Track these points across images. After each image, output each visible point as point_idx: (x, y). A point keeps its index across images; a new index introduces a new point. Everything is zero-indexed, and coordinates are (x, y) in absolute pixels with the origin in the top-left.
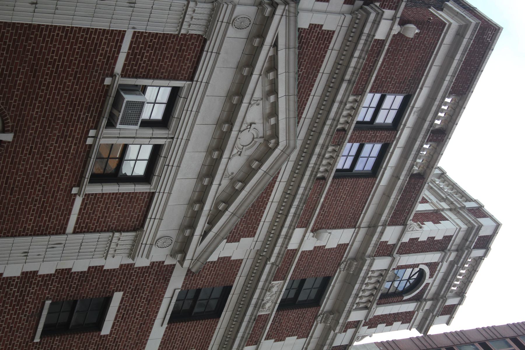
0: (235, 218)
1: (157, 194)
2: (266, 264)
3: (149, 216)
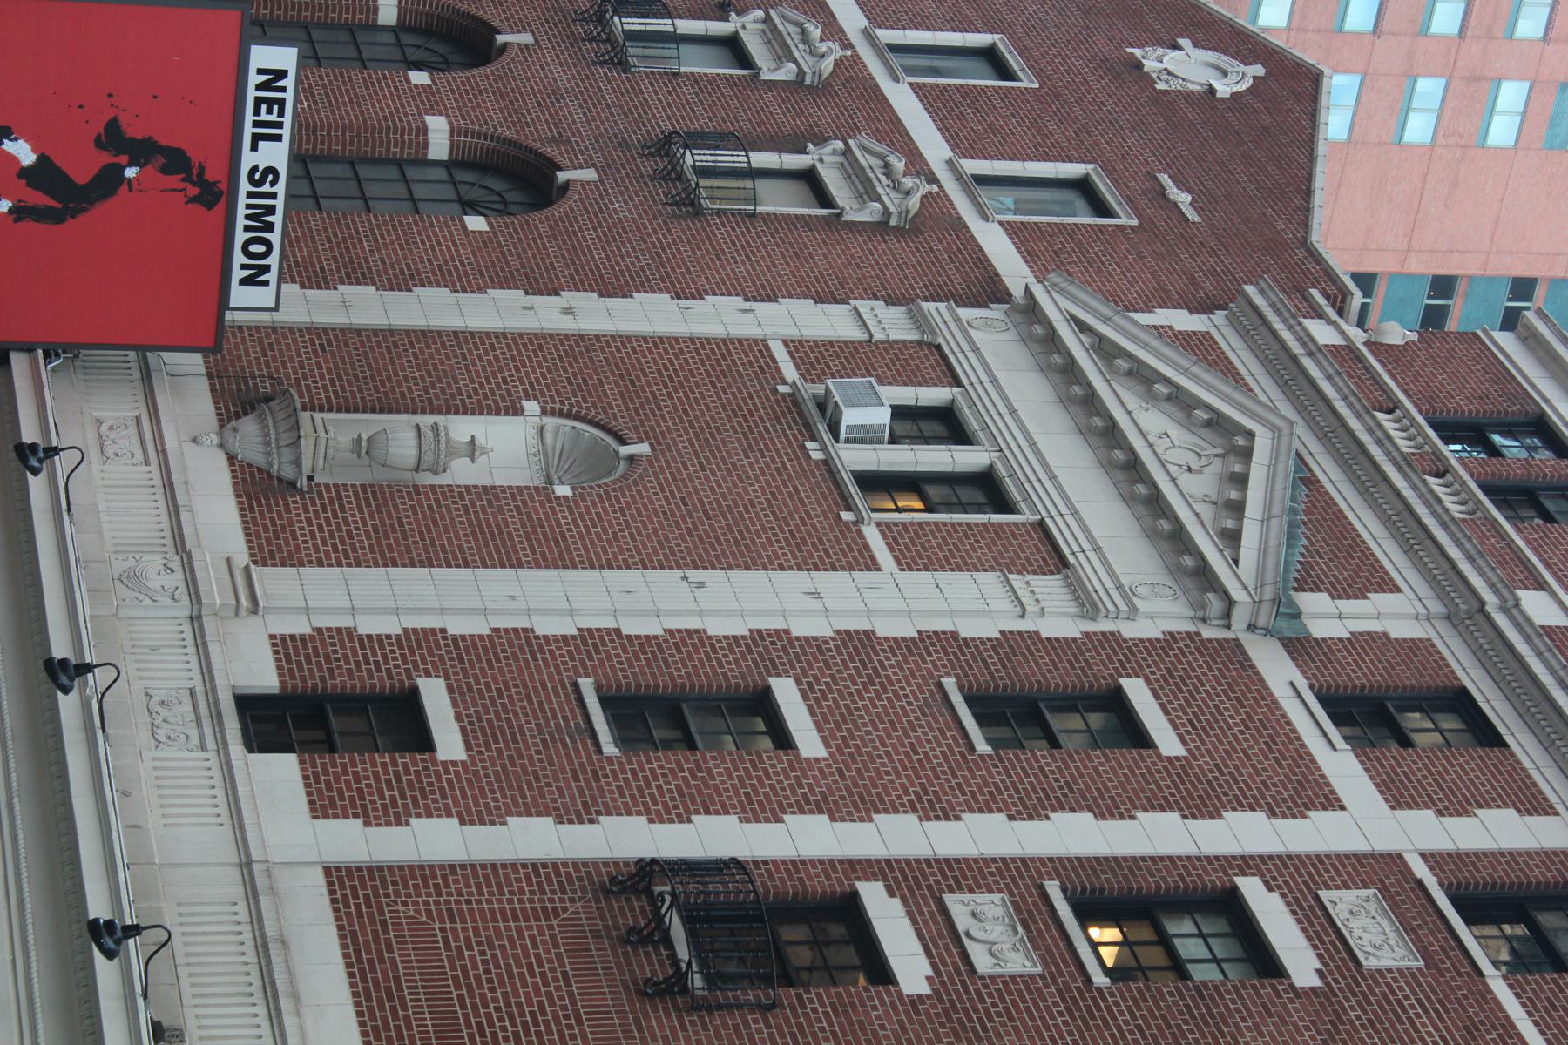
0: (1274, 522)
1: (1049, 522)
2: (1488, 617)
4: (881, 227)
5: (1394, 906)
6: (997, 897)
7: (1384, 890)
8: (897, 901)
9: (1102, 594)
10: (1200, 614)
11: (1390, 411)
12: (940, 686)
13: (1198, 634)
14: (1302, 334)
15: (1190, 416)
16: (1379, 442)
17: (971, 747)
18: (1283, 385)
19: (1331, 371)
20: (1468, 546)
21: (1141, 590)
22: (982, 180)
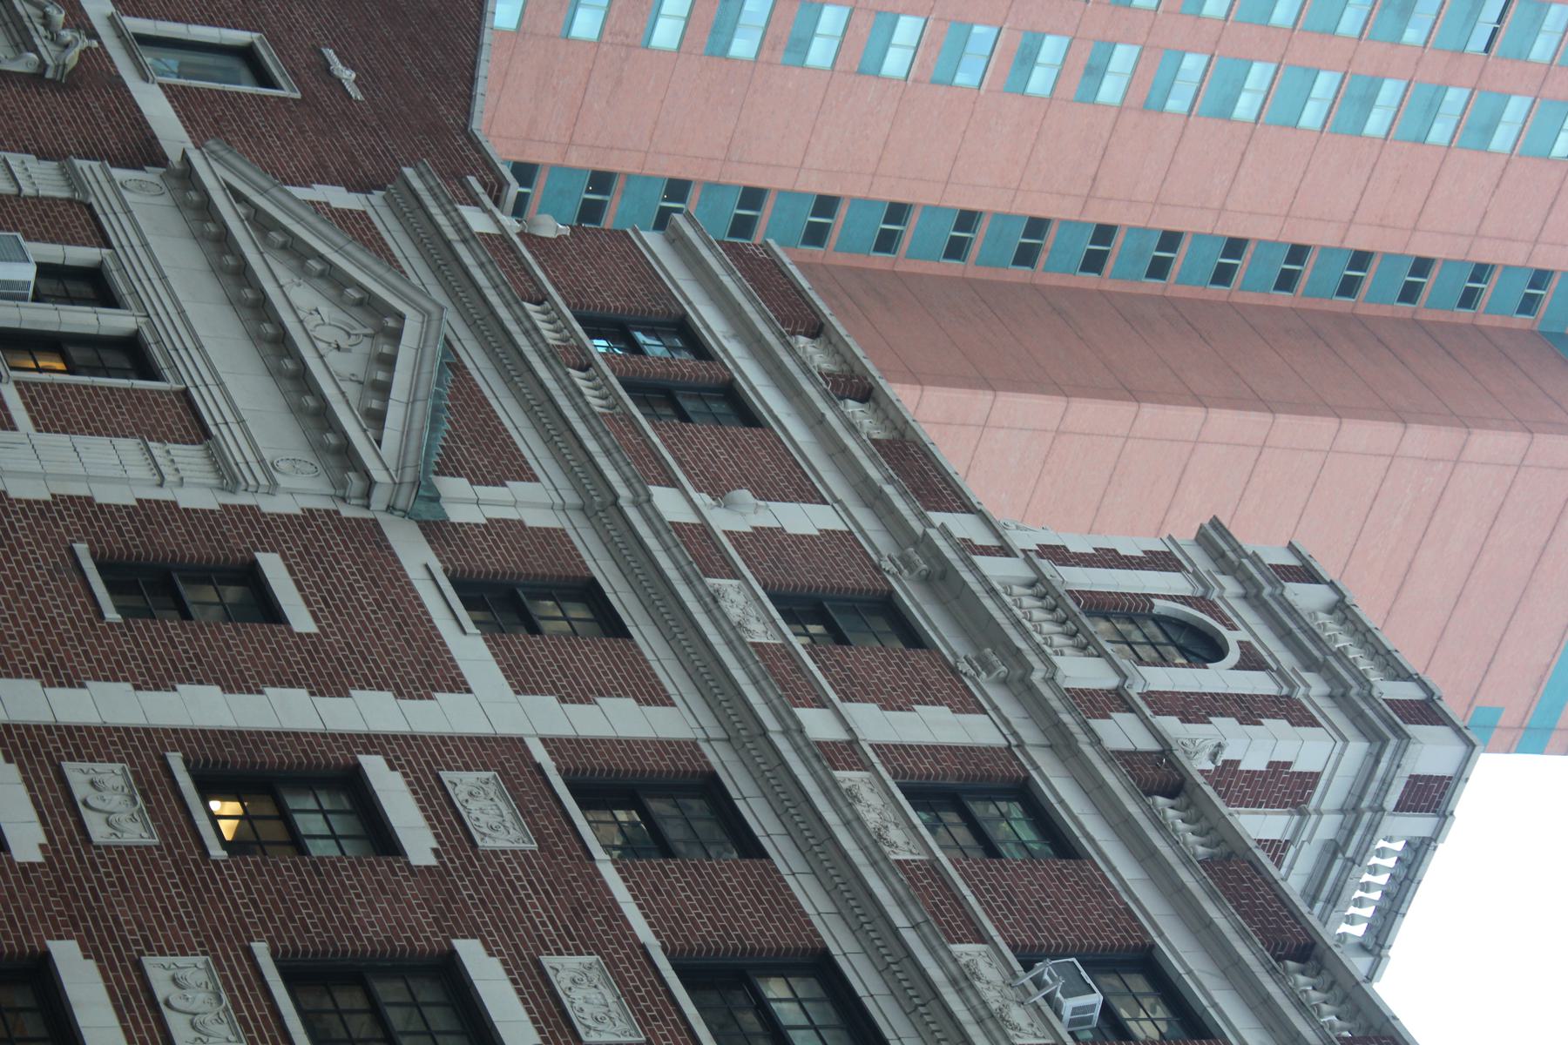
0: (419, 406)
1: (193, 391)
2: (621, 511)
3: (209, 421)
4: (37, 78)
5: (513, 789)
6: (117, 767)
7: (504, 773)
8: (13, 767)
9: (243, 467)
10: (340, 493)
11: (539, 303)
12: (71, 551)
13: (337, 512)
14: (457, 220)
15: (341, 294)
16: (526, 333)
17: (100, 615)
18: (436, 270)
19: (484, 259)
20: (606, 440)
21: (282, 466)
22: (145, 40)
